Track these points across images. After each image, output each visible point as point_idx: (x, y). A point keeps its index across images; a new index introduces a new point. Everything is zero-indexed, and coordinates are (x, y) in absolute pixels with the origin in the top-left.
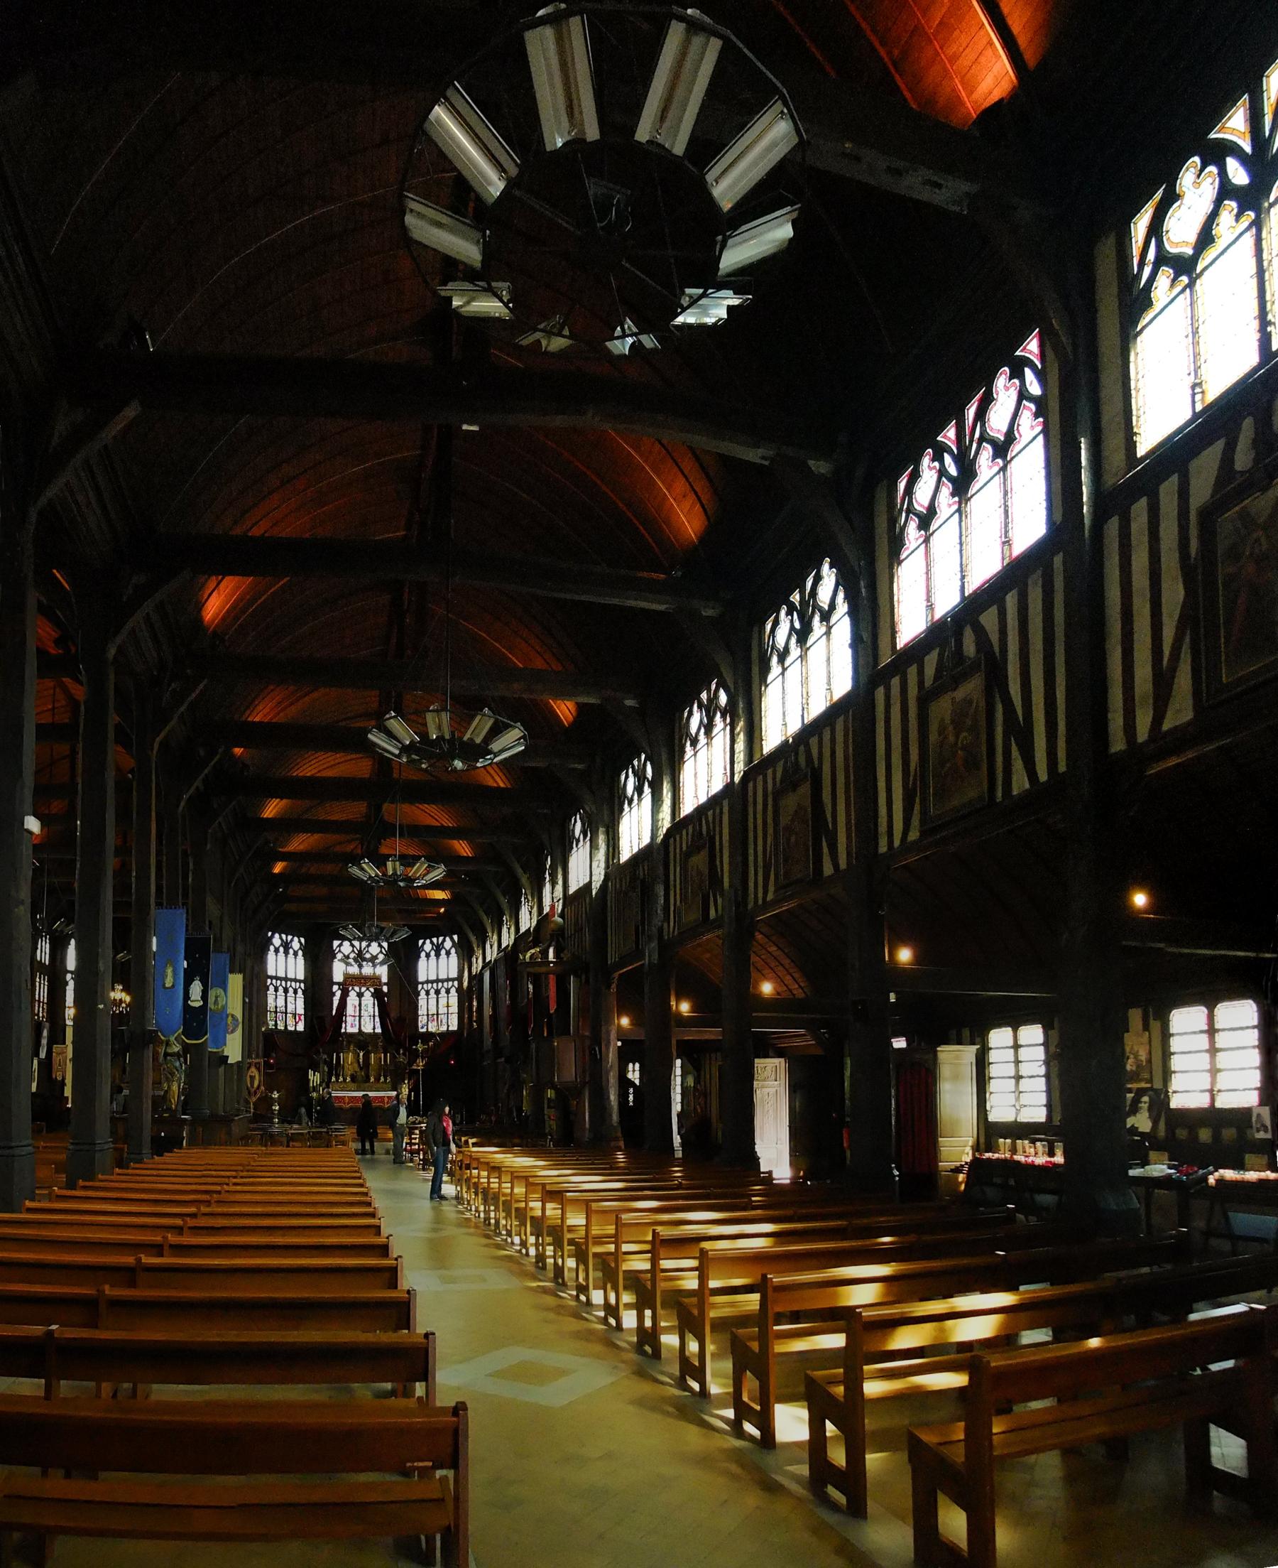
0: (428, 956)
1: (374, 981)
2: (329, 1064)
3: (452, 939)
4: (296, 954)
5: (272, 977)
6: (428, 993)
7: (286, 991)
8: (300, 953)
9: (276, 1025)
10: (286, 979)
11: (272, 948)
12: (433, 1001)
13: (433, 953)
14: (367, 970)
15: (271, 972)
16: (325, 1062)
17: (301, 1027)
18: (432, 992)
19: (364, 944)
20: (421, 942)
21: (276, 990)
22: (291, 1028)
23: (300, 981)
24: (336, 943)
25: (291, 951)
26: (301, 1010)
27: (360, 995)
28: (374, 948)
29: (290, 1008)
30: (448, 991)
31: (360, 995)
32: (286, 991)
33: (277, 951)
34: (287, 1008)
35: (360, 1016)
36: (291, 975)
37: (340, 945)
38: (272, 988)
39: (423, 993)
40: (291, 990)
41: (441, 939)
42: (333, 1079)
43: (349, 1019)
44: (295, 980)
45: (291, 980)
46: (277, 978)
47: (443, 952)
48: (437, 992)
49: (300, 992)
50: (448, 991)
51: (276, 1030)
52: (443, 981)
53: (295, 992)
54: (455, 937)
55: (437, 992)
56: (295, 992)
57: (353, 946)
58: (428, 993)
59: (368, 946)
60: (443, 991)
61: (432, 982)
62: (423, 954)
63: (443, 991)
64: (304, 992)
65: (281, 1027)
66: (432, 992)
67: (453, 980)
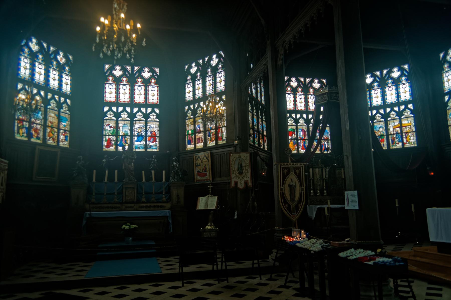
5: (23, 81)
9: (30, 136)
24: (107, 67)
26: (65, 125)
33: (33, 56)
35: (132, 136)
40: (53, 104)
45: (53, 92)
56: (59, 105)
59: (141, 70)
64: (70, 108)
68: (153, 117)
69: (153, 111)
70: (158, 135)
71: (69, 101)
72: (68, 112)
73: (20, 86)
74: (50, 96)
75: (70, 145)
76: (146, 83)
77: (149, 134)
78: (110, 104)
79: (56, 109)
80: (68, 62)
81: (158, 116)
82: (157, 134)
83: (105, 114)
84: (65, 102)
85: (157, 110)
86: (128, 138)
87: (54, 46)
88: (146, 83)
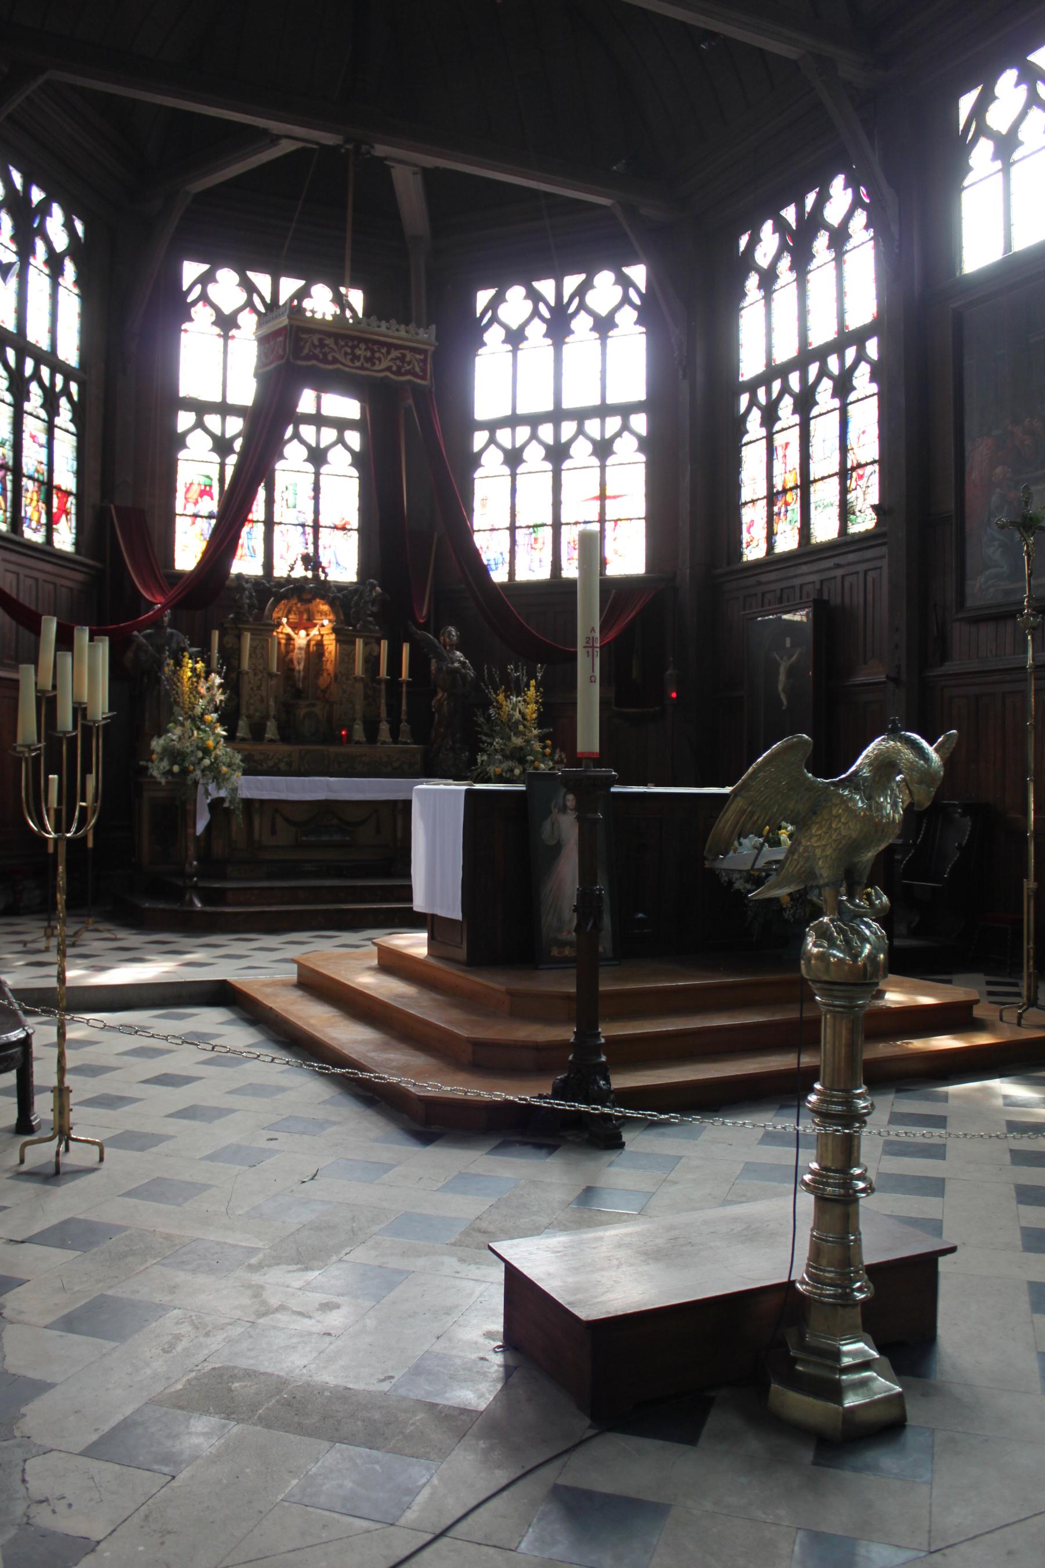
0: (515, 338)
3: (625, 282)
4: (55, 264)
6: (513, 458)
8: (70, 268)
13: (537, 329)
17: (65, 539)
18: (534, 455)
20: (483, 297)
24: (191, 270)
25: (40, 246)
29: (33, 458)
30: (603, 449)
36: (37, 335)
37: (206, 279)
39: (492, 462)
41: (572, 282)
47: (582, 323)
48: (557, 454)
50: (603, 449)
52: (581, 415)
54: (638, 273)
55: (557, 454)
56: (51, 405)
58: (513, 458)
60: (581, 450)
61: (534, 421)
62: (494, 336)
63: (581, 450)
66: (534, 455)
67: (625, 411)
68: (340, 461)
69: (341, 440)
71: (74, 387)
72: (72, 428)
74: (29, 365)
75: (77, 544)
77: (323, 521)
78: (201, 408)
79: (43, 414)
80: (75, 249)
81: (359, 460)
82: (354, 520)
83: (179, 442)
84: (66, 391)
85: (354, 439)
87: (42, 188)
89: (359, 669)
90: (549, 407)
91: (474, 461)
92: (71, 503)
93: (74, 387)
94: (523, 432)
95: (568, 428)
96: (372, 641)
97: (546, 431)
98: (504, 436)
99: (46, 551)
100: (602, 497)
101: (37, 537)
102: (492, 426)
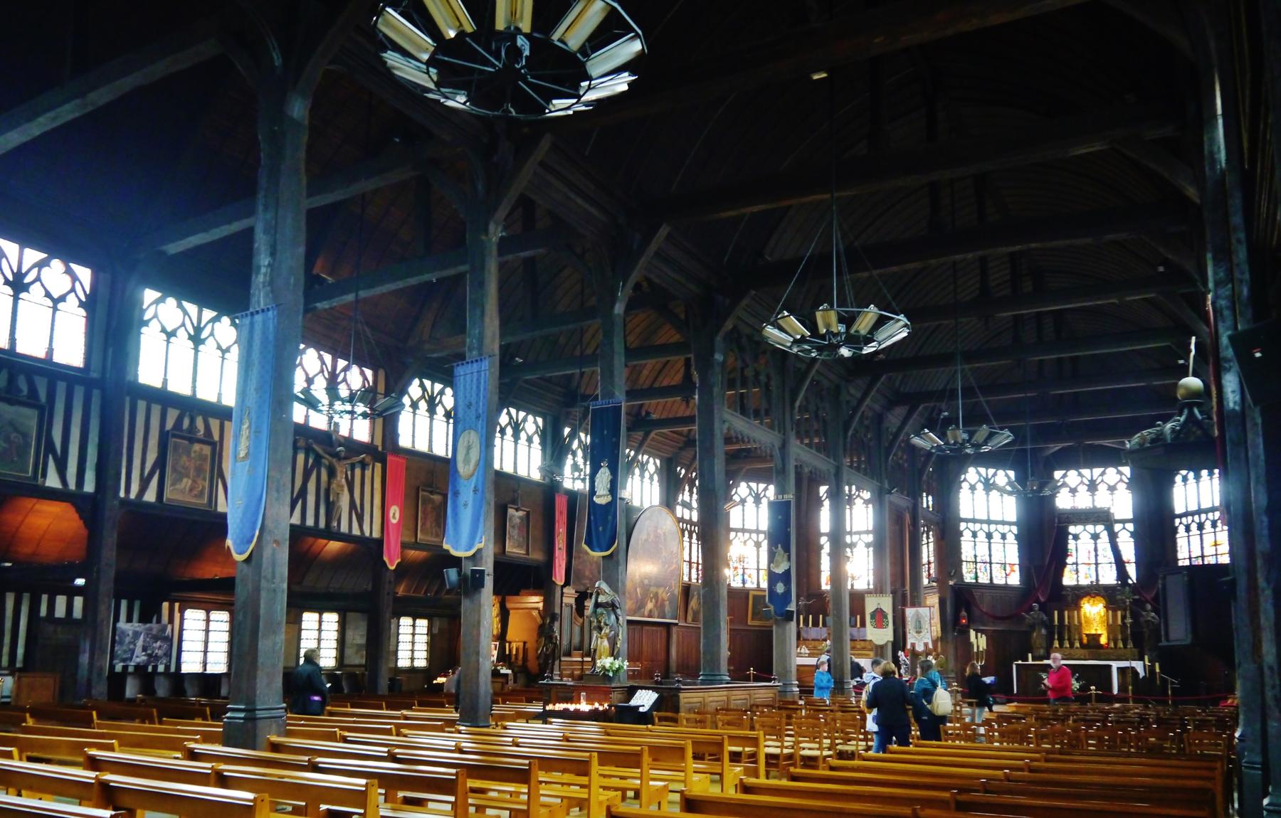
1: (1102, 517)
2: (1049, 626)
5: (967, 521)
6: (1188, 529)
7: (989, 536)
9: (976, 578)
10: (989, 522)
11: (965, 485)
12: (1195, 540)
14: (1102, 500)
15: (965, 512)
16: (1043, 624)
17: (1015, 580)
18: (1194, 527)
19: (1097, 471)
21: (974, 535)
22: (999, 580)
23: (1010, 524)
24: (1058, 474)
27: (1095, 537)
28: (1111, 475)
31: (1095, 537)
32: (989, 536)
33: (973, 488)
34: (993, 557)
35: (1097, 564)
38: (967, 536)
39: (1181, 529)
40: (997, 537)
42: (1056, 644)
43: (1082, 568)
44: (1003, 523)
45: (997, 523)
46: (974, 521)
48: (1201, 527)
49: (1011, 538)
51: (977, 586)
53: (1004, 537)
55: (1201, 527)
56: (1004, 537)
57: (1080, 475)
58: (1188, 529)
59: (1103, 474)
61: (1193, 514)
63: (1208, 525)
64: (1017, 537)
65: (984, 579)
66: (1194, 527)
70: (1133, 559)
73: (963, 526)
76: (1112, 489)
81: (1133, 535)
85: (1130, 527)
86: (1093, 567)
88: (1112, 489)
89: (1119, 622)
90: (1196, 508)
91: (1175, 530)
92: (1017, 568)
93: (1015, 529)
94: (1190, 518)
95: (1203, 516)
96: (1115, 611)
97: (1196, 518)
98: (1184, 520)
99: (1006, 587)
100: (1216, 545)
101: (1002, 582)
102: (1180, 516)
